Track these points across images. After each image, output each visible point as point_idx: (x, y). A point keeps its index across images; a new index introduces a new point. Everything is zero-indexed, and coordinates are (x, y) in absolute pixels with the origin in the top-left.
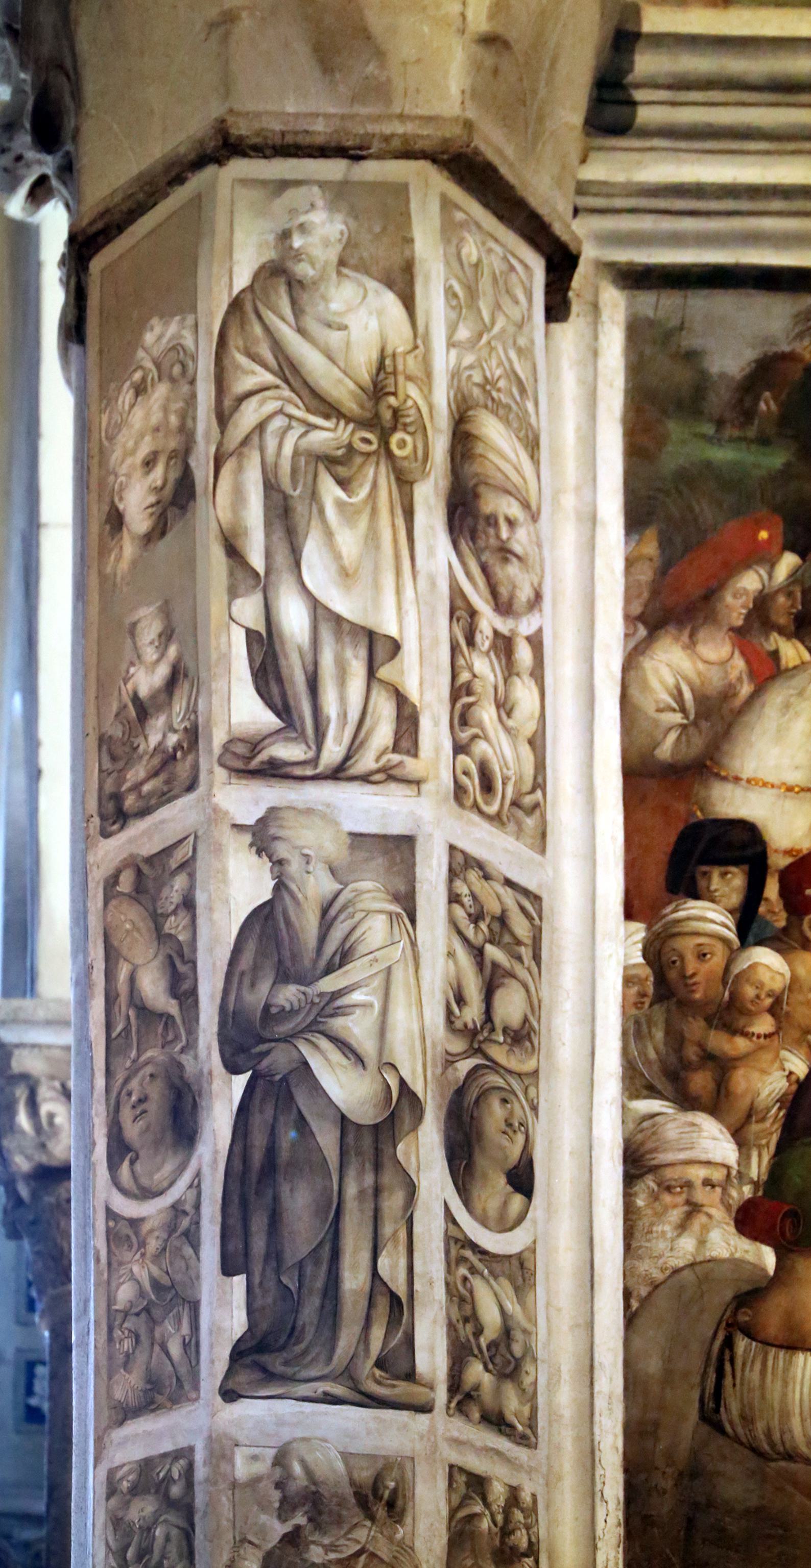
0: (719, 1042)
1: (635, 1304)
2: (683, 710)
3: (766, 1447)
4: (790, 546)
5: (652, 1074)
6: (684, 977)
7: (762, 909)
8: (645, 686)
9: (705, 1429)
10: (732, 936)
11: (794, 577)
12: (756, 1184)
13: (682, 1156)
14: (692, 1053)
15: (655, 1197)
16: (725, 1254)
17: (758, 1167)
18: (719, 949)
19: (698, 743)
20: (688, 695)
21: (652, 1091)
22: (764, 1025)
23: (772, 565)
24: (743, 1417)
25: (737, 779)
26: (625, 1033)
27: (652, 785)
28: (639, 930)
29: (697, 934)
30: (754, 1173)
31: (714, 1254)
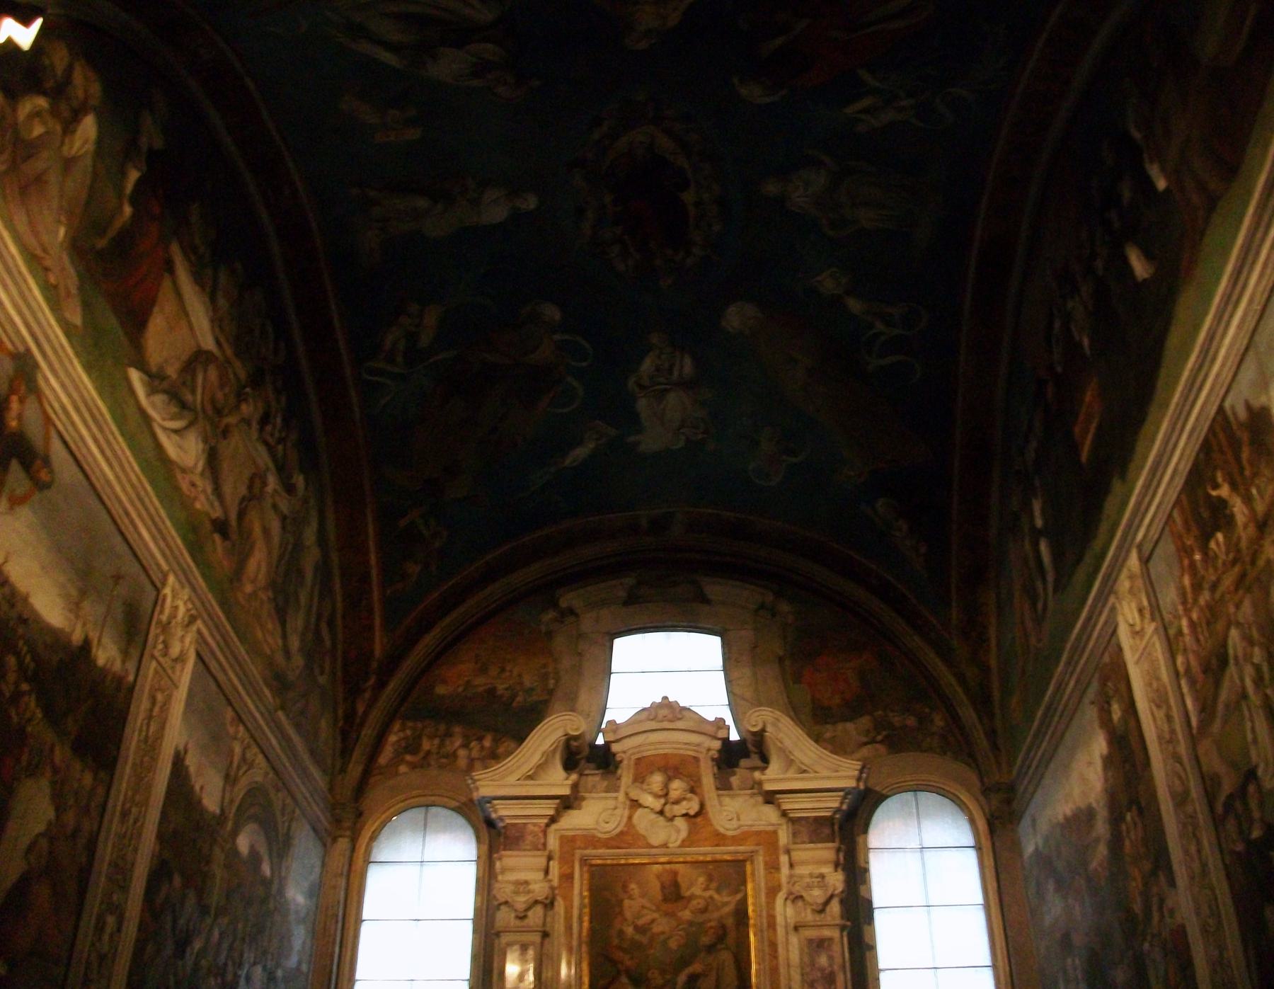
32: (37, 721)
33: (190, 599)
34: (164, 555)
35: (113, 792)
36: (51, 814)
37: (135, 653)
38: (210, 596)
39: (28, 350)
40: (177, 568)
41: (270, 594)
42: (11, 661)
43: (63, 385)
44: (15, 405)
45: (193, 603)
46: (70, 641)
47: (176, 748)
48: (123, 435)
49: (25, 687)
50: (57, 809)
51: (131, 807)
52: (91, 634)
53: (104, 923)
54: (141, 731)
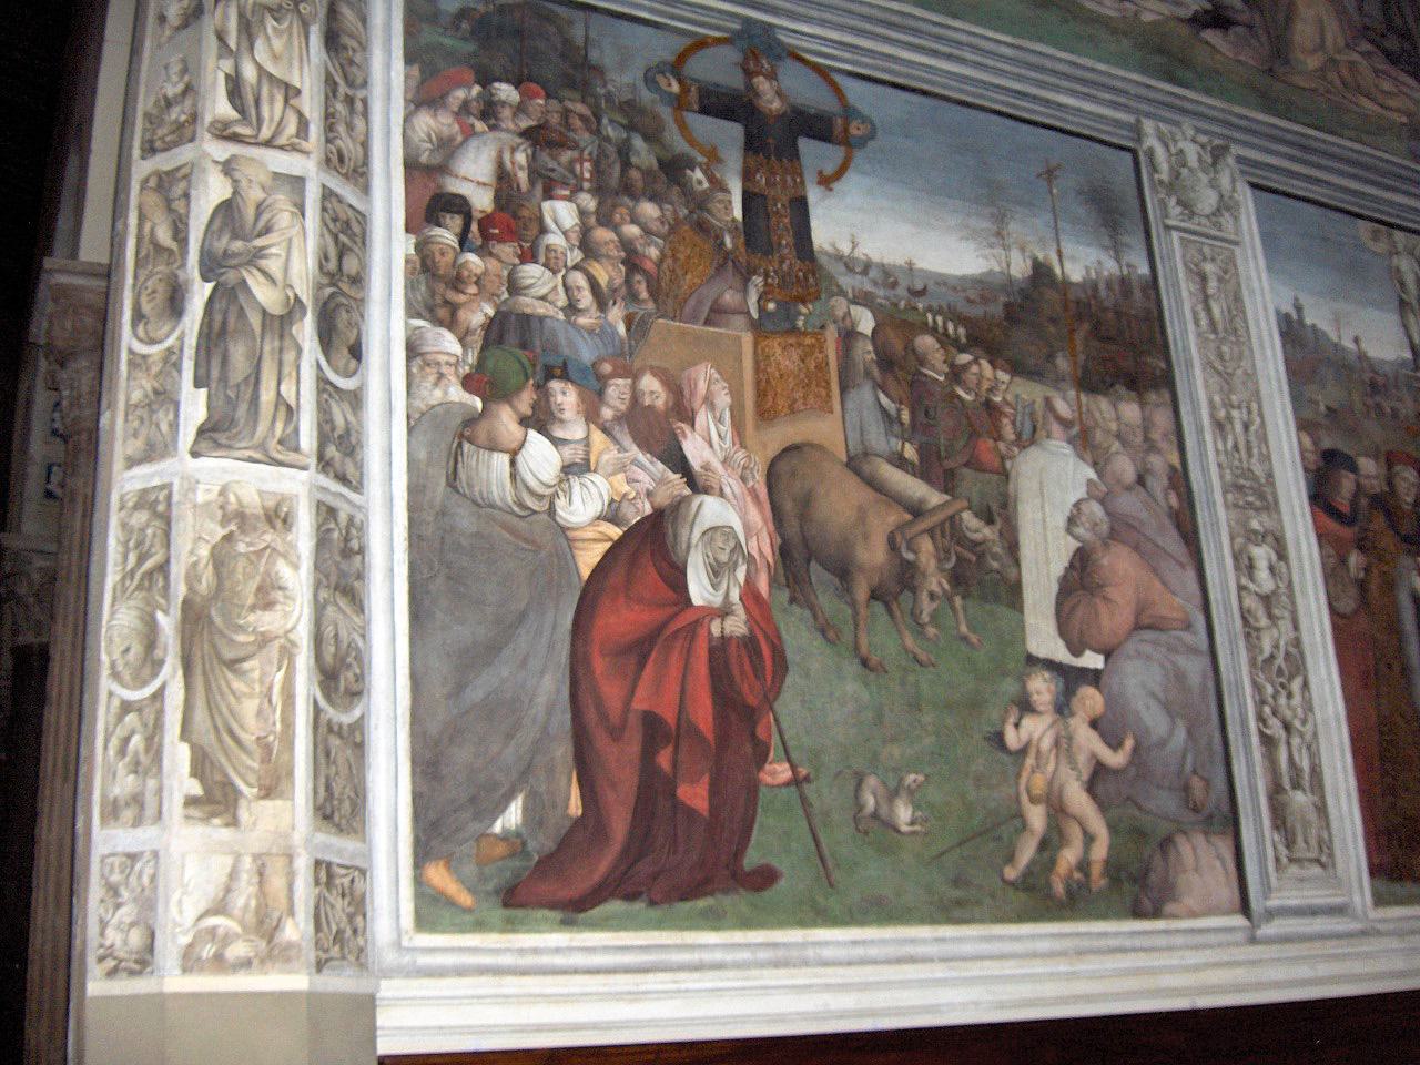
0: (452, 296)
1: (412, 422)
2: (431, 141)
3: (480, 501)
4: (479, 83)
5: (420, 307)
6: (433, 261)
7: (470, 236)
8: (413, 129)
9: (449, 489)
10: (457, 246)
11: (479, 95)
12: (471, 366)
13: (435, 349)
14: (439, 300)
15: (422, 368)
16: (457, 400)
17: (472, 358)
18: (450, 251)
19: (437, 159)
20: (433, 136)
21: (419, 316)
22: (473, 289)
23: (470, 88)
24: (468, 484)
25: (457, 176)
26: (406, 287)
27: (417, 174)
28: (412, 239)
29: (440, 243)
30: (470, 361)
31: (452, 399)
32: (1004, 387)
33: (1198, 130)
34: (1115, 105)
35: (1184, 409)
36: (1092, 474)
37: (1135, 241)
38: (1237, 109)
39: (747, 21)
40: (1144, 107)
41: (1366, 46)
42: (926, 342)
43: (823, 23)
44: (762, 84)
45: (1205, 132)
46: (1010, 279)
47: (1278, 312)
48: (955, 16)
49: (964, 358)
50: (1095, 465)
51: (1228, 413)
52: (1041, 256)
53: (1250, 559)
54: (1197, 322)
